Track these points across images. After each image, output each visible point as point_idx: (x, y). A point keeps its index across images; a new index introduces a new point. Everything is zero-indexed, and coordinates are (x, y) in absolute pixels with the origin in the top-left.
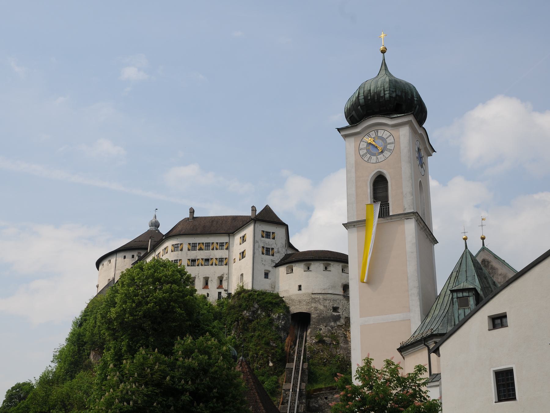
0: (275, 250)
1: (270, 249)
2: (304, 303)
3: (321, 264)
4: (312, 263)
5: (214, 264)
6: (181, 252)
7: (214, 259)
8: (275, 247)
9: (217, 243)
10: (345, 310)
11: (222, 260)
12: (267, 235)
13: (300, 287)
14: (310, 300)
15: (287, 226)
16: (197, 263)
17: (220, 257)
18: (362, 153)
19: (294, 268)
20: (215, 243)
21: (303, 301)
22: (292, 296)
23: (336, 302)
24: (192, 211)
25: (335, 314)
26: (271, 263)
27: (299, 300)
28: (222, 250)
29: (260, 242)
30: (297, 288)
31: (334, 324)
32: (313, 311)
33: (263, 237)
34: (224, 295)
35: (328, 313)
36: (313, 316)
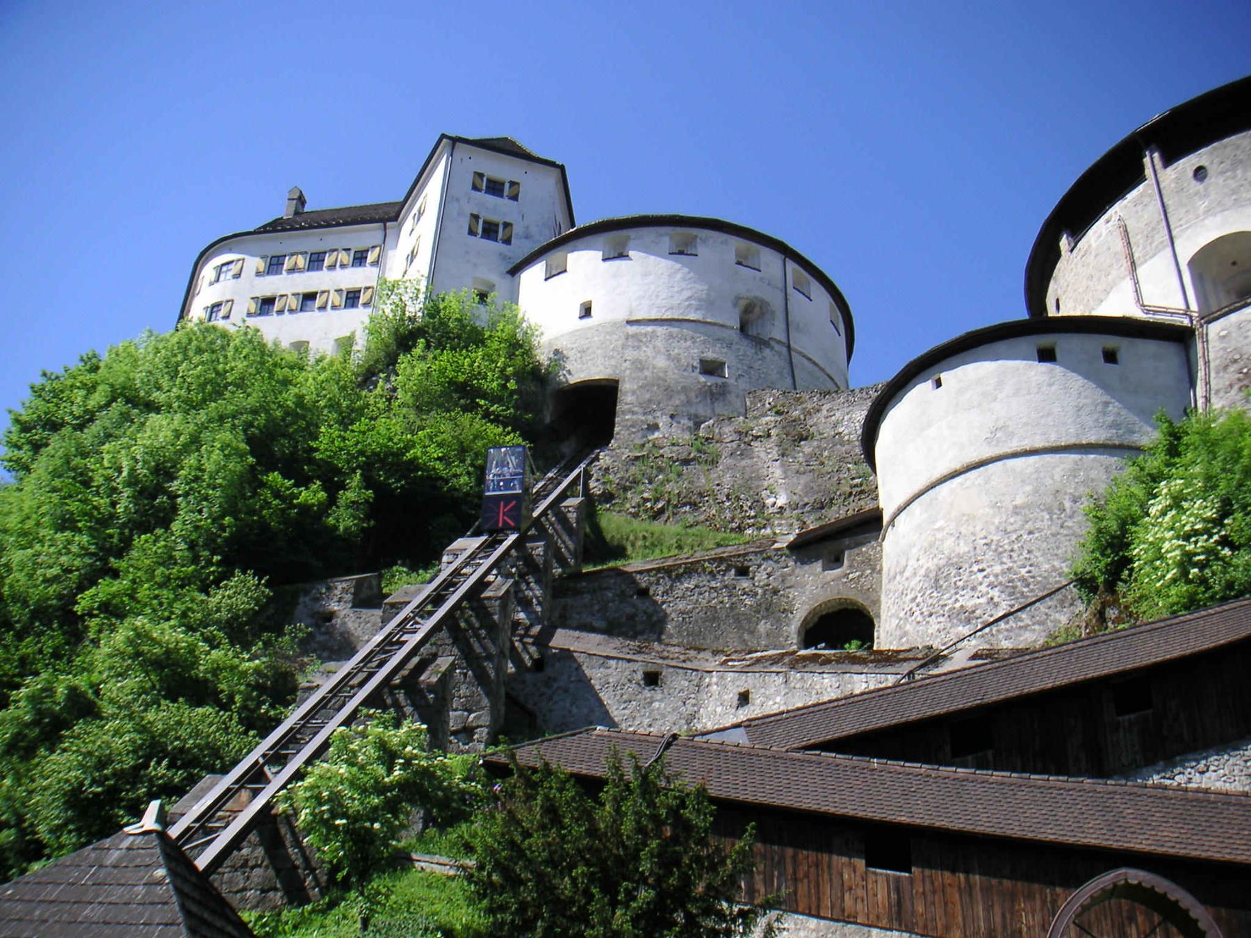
0: (517, 229)
1: (497, 225)
3: (661, 235)
12: (495, 188)
13: (587, 311)
15: (562, 168)
16: (277, 306)
22: (556, 339)
30: (577, 312)
32: (628, 372)
33: (475, 188)
36: (626, 387)
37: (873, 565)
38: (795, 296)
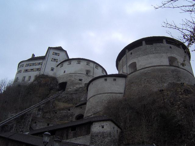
12: (56, 54)
24: (33, 55)
30: (63, 72)
33: (53, 54)
36: (68, 83)
37: (85, 109)
38: (95, 69)
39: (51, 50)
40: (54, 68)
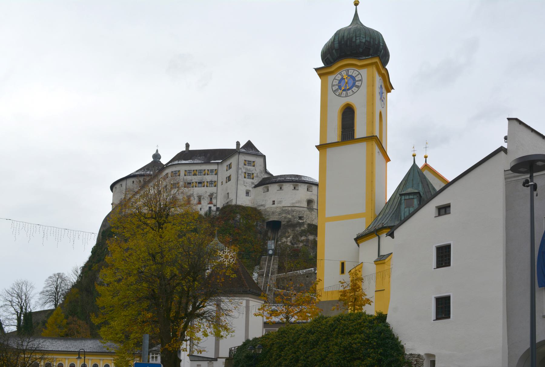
0: (255, 175)
1: (250, 174)
2: (277, 214)
3: (291, 185)
4: (284, 184)
5: (205, 186)
6: (179, 177)
7: (206, 182)
8: (255, 172)
9: (208, 170)
10: (308, 218)
11: (212, 183)
12: (249, 163)
13: (274, 201)
14: (281, 212)
17: (210, 181)
18: (334, 89)
19: (270, 189)
20: (206, 170)
21: (276, 212)
23: (302, 213)
25: (300, 221)
26: (251, 184)
27: (273, 212)
28: (212, 176)
29: (243, 169)
30: (272, 203)
31: (299, 228)
33: (245, 165)
34: (214, 208)
35: (295, 221)
36: (283, 223)
39: (240, 156)
40: (250, 191)
